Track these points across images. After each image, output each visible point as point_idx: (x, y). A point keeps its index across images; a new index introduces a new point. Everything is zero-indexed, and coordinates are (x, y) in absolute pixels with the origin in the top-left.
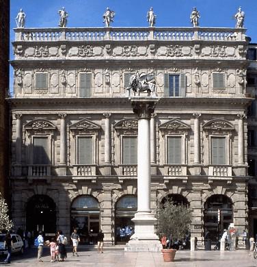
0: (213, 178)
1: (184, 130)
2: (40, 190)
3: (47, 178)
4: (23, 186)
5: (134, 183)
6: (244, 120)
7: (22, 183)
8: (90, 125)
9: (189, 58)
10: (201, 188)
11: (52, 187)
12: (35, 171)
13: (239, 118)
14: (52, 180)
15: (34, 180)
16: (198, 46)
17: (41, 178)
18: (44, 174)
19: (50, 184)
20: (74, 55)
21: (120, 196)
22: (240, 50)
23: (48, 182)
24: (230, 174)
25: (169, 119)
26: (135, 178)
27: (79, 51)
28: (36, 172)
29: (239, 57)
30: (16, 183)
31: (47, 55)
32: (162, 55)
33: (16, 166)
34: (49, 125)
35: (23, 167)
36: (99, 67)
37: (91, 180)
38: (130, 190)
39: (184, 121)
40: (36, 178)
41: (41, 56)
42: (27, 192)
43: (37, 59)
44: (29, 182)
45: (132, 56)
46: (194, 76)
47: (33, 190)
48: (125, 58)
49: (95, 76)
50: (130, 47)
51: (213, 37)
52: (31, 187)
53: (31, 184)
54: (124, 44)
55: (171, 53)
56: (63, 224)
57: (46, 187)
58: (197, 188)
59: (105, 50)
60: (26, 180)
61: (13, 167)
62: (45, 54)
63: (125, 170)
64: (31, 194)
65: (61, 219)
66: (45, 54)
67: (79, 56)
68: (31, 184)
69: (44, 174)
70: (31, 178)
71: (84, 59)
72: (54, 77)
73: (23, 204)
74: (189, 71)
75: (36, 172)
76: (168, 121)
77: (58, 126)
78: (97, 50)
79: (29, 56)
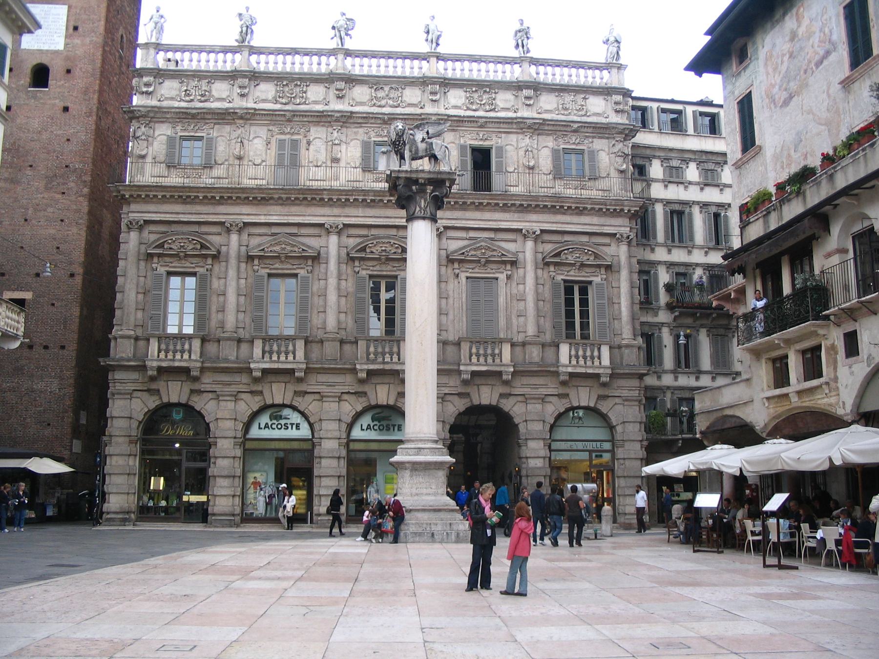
0: (570, 370)
1: (504, 263)
2: (175, 392)
3: (191, 365)
4: (135, 381)
5: (397, 377)
6: (629, 244)
7: (134, 375)
8: (294, 246)
9: (511, 114)
10: (543, 391)
11: (203, 387)
12: (163, 346)
13: (619, 241)
14: (203, 370)
15: (160, 369)
16: (530, 93)
17: (177, 364)
18: (186, 356)
19: (196, 379)
20: (264, 101)
21: (359, 408)
22: (616, 103)
23: (194, 373)
24: (606, 361)
25: (471, 239)
26: (398, 367)
27: (277, 91)
28: (167, 351)
29: (615, 119)
30: (119, 375)
31: (205, 97)
32: (456, 107)
33: (123, 337)
34: (203, 246)
35: (137, 339)
36: (317, 123)
37: (292, 371)
38: (382, 395)
39: (503, 245)
40: (164, 364)
41: (192, 101)
42: (145, 395)
43: (183, 104)
44: (150, 373)
45: (391, 107)
46: (522, 153)
47: (157, 392)
48: (375, 110)
49: (309, 143)
50: (387, 88)
51: (562, 76)
52: (154, 386)
53: (153, 379)
54: (375, 82)
55: (472, 103)
56: (226, 473)
57: (187, 387)
58: (534, 392)
59: (332, 93)
60: (143, 368)
61: (115, 339)
62: (202, 95)
63: (372, 349)
64: (153, 403)
65: (221, 462)
66: (202, 95)
67: (276, 102)
68: (153, 379)
69: (186, 356)
70: (155, 364)
71: (287, 107)
72: (224, 140)
73: (135, 424)
74: (513, 137)
75: (167, 351)
76: (466, 243)
77: (224, 249)
78: (315, 92)
79: (167, 99)
